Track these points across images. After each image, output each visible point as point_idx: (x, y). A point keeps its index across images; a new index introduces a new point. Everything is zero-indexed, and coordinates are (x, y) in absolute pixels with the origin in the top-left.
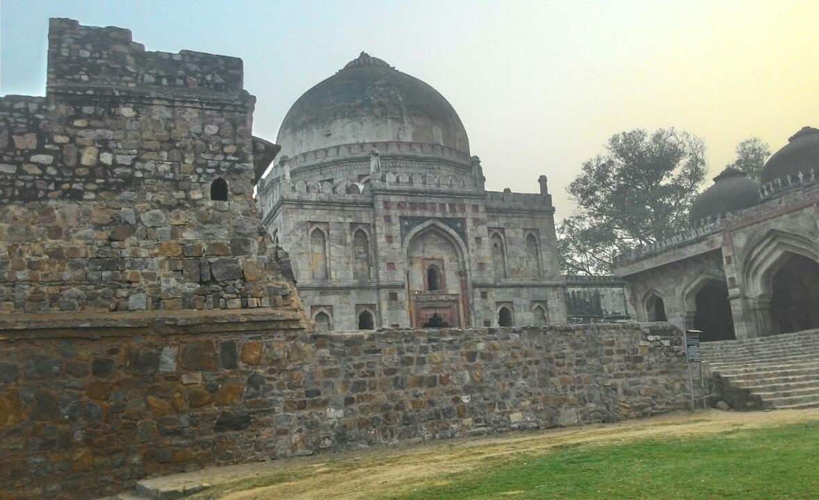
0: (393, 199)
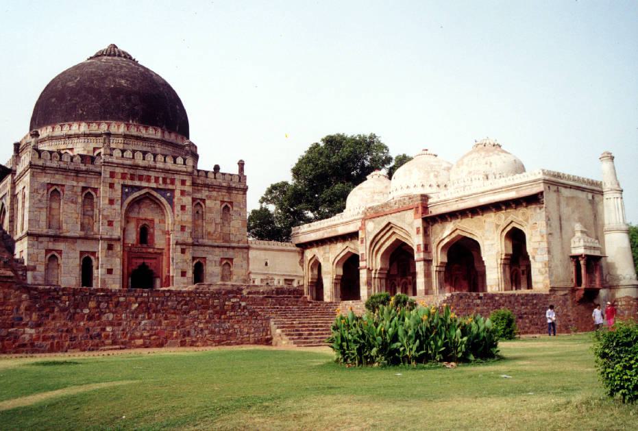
0: (119, 170)
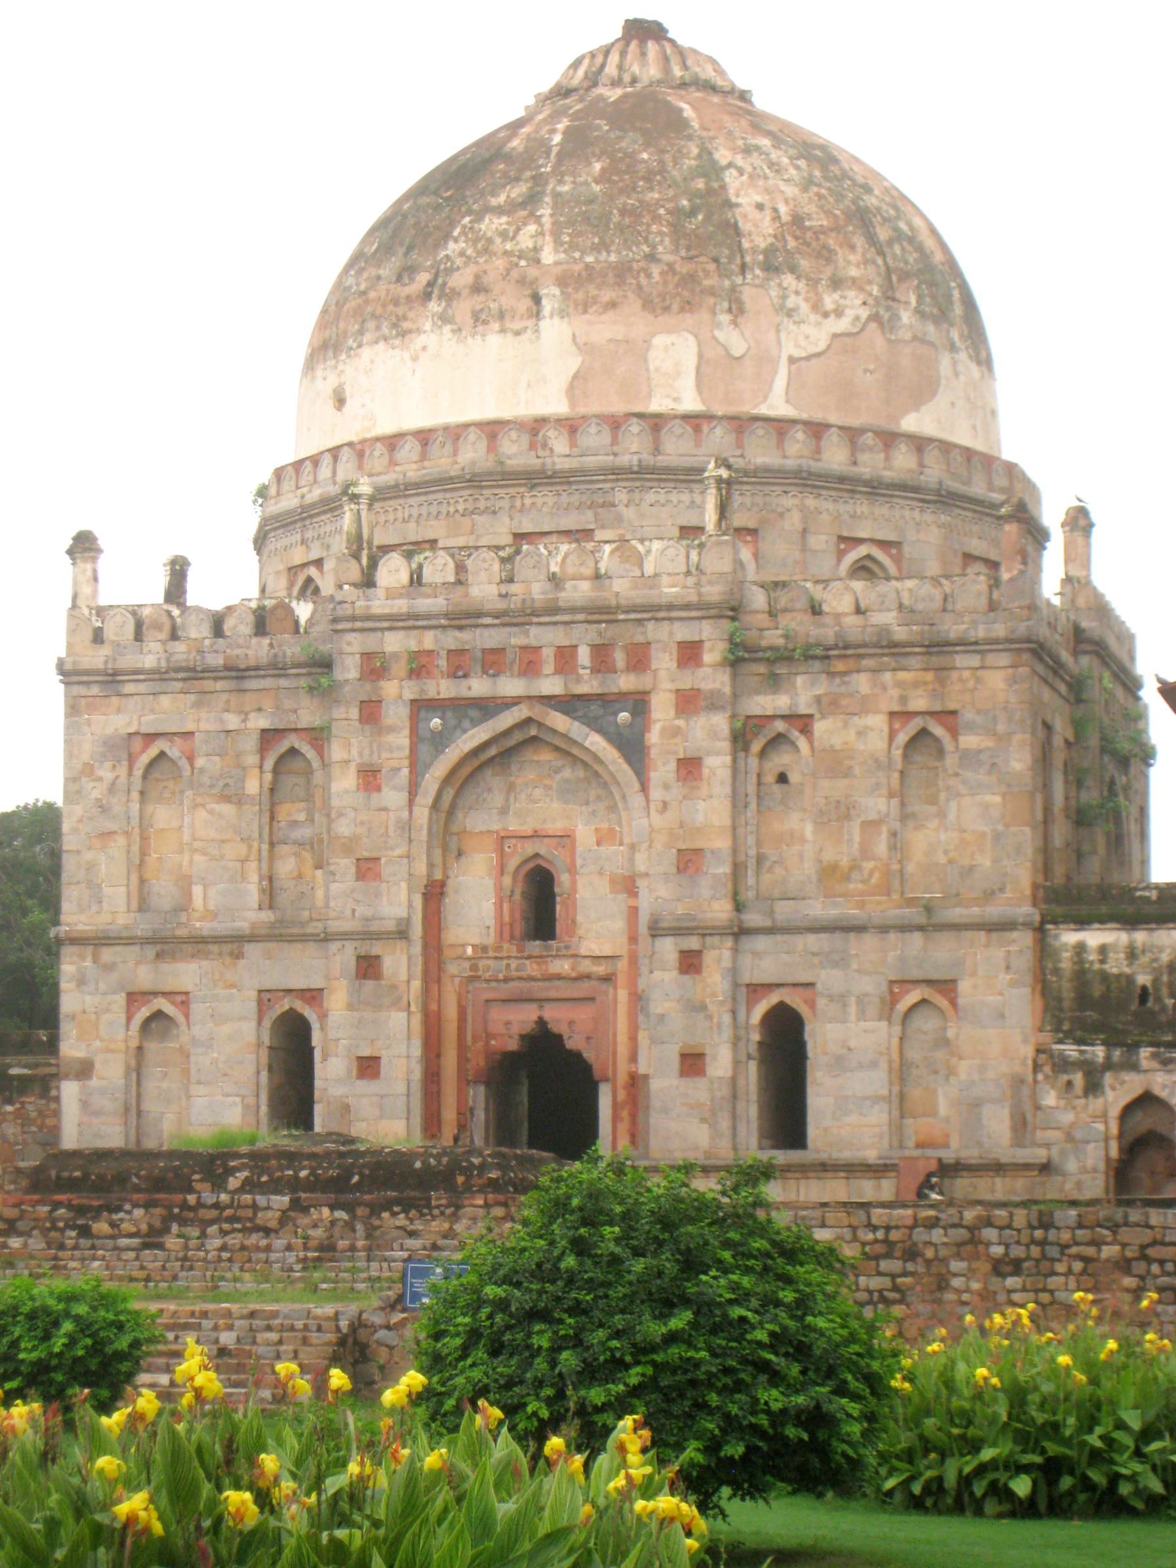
0: (394, 643)
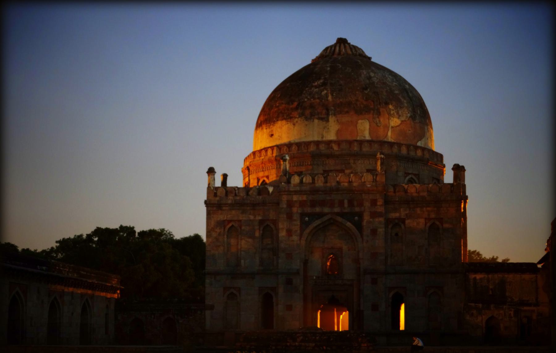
0: (295, 198)
